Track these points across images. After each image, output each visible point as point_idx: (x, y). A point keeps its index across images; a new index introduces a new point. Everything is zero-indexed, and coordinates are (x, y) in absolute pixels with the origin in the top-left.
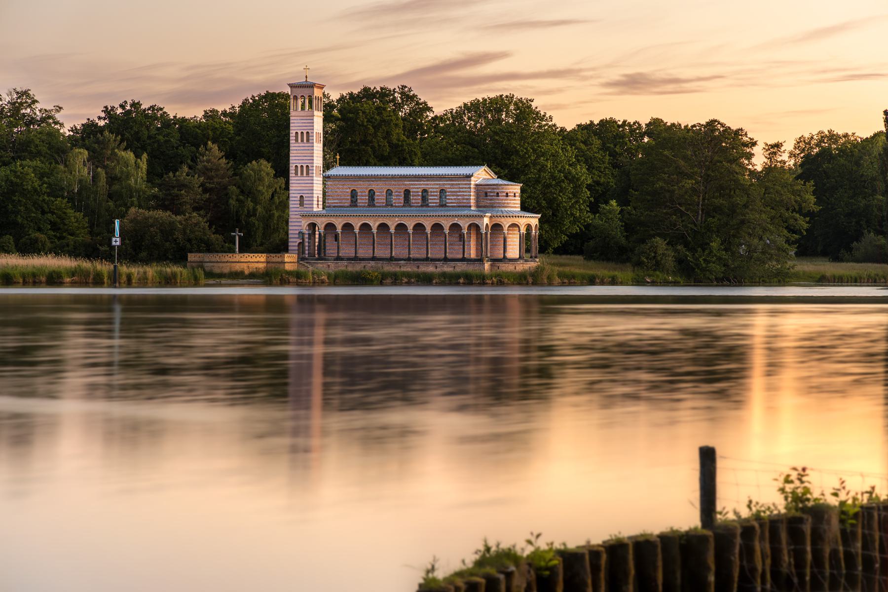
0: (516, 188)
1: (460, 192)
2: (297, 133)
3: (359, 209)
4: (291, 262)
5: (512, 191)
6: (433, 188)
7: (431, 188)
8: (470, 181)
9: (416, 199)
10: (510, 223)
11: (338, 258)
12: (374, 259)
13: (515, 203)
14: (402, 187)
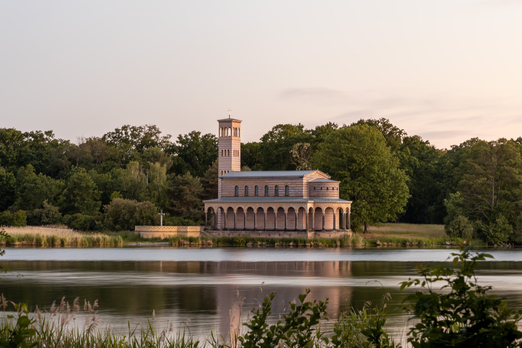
0: (336, 184)
2: (222, 150)
3: (239, 198)
4: (193, 232)
5: (331, 186)
6: (282, 184)
7: (281, 185)
8: (303, 180)
9: (271, 192)
10: (327, 207)
11: (225, 229)
12: (244, 229)
13: (335, 194)
14: (264, 184)
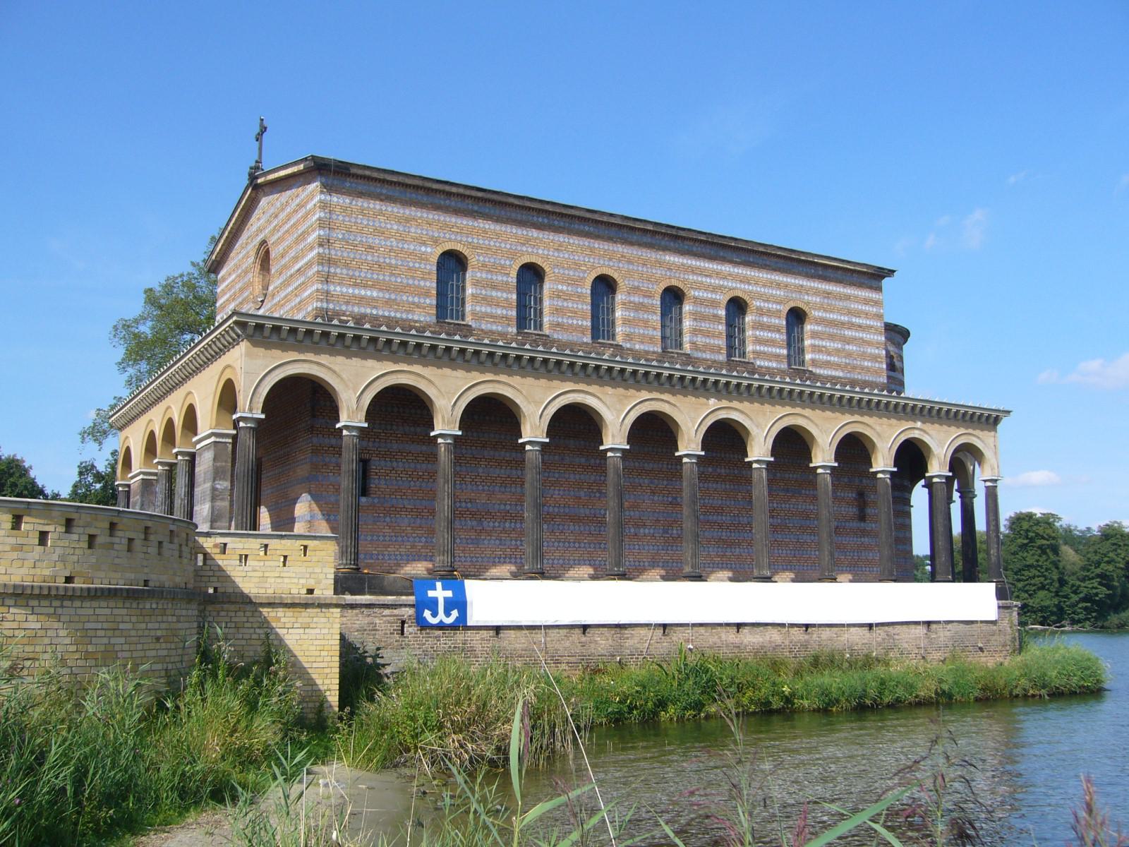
1: (851, 326)
7: (760, 296)
9: (707, 334)
14: (658, 272)
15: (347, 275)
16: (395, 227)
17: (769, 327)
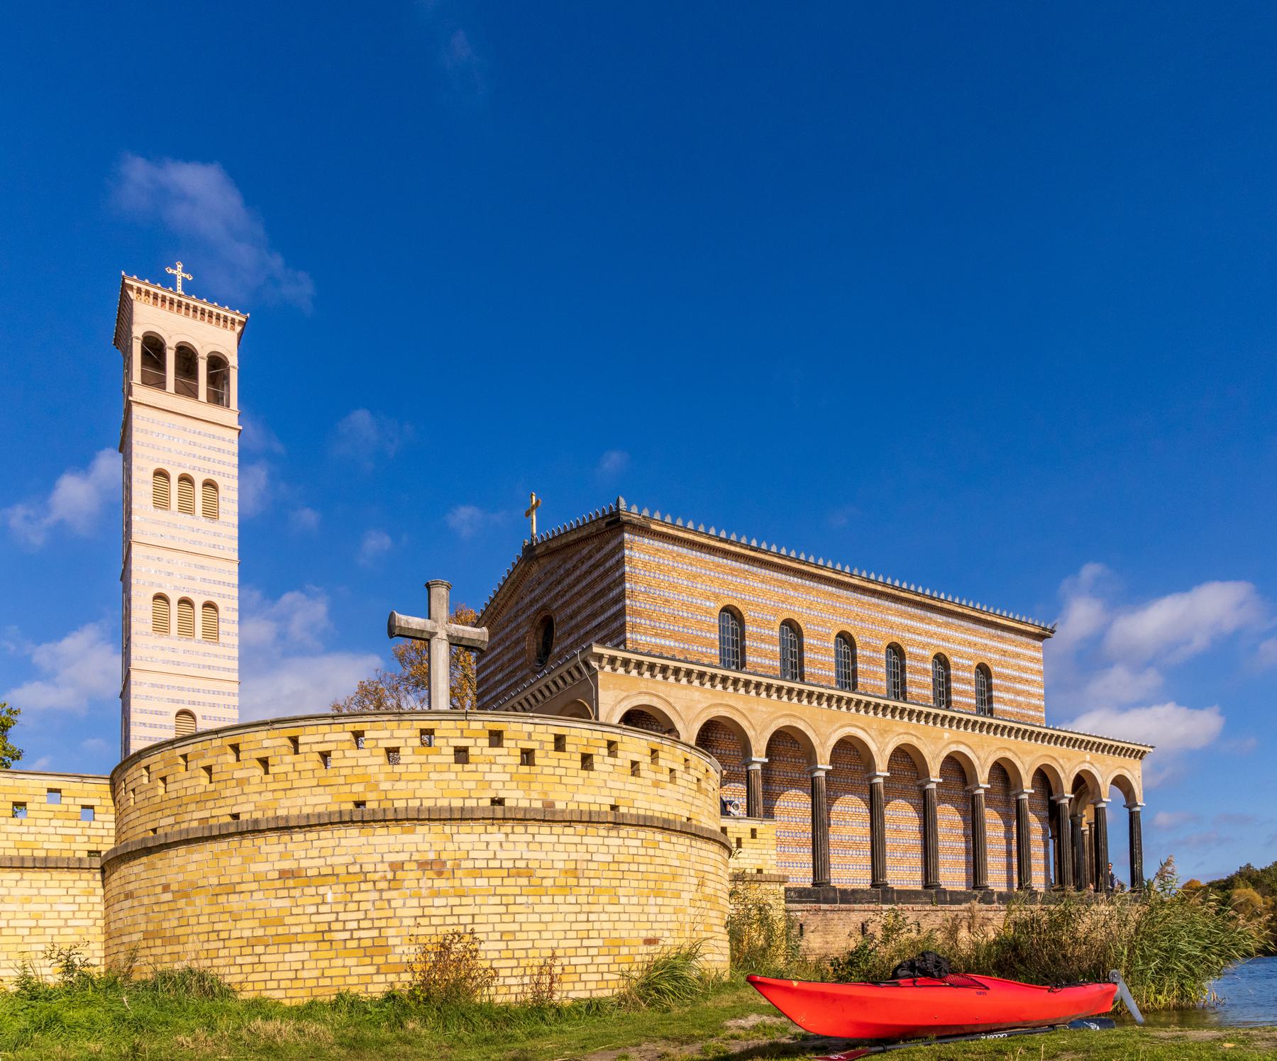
14: (884, 630)
15: (650, 625)
16: (685, 583)
17: (963, 680)
